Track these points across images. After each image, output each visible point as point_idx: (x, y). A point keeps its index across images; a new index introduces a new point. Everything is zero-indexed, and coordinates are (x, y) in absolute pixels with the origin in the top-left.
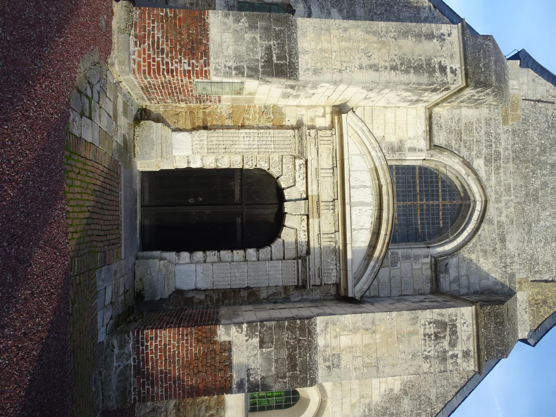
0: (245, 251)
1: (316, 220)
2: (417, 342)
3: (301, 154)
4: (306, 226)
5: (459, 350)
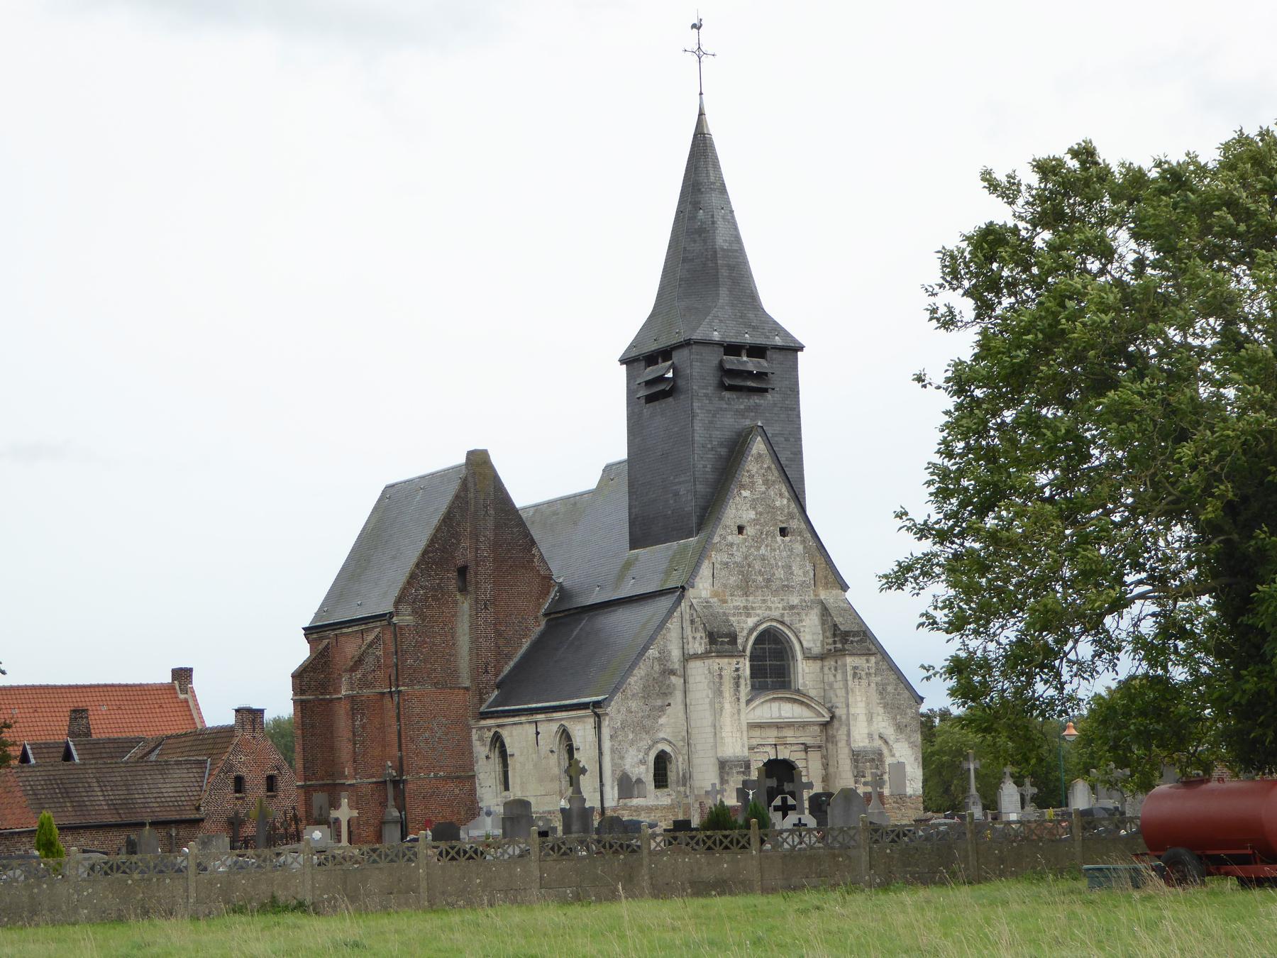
5: (865, 665)
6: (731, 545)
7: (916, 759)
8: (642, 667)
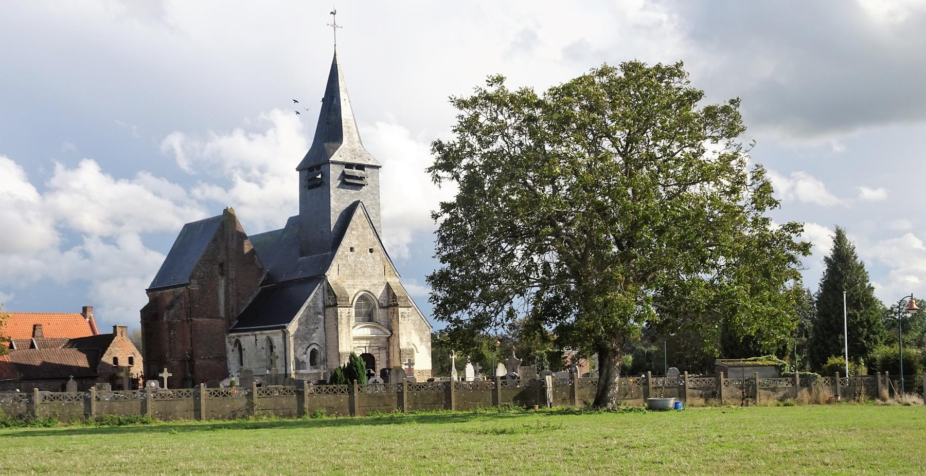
2: (406, 322)
5: (407, 312)
6: (347, 256)
7: (429, 354)
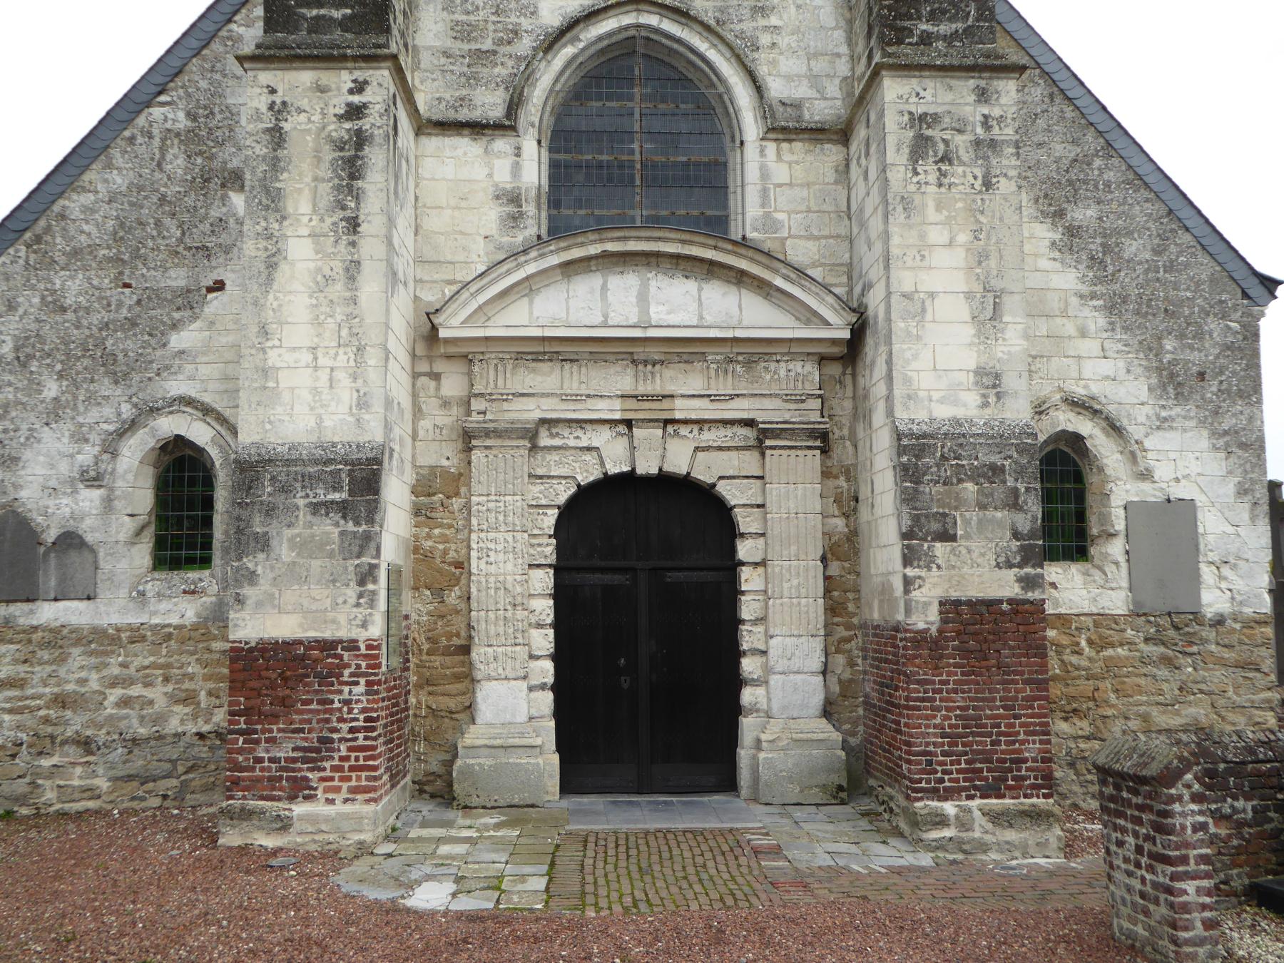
0: (743, 564)
1: (678, 403)
3: (530, 435)
4: (689, 427)
8: (119, 160)
